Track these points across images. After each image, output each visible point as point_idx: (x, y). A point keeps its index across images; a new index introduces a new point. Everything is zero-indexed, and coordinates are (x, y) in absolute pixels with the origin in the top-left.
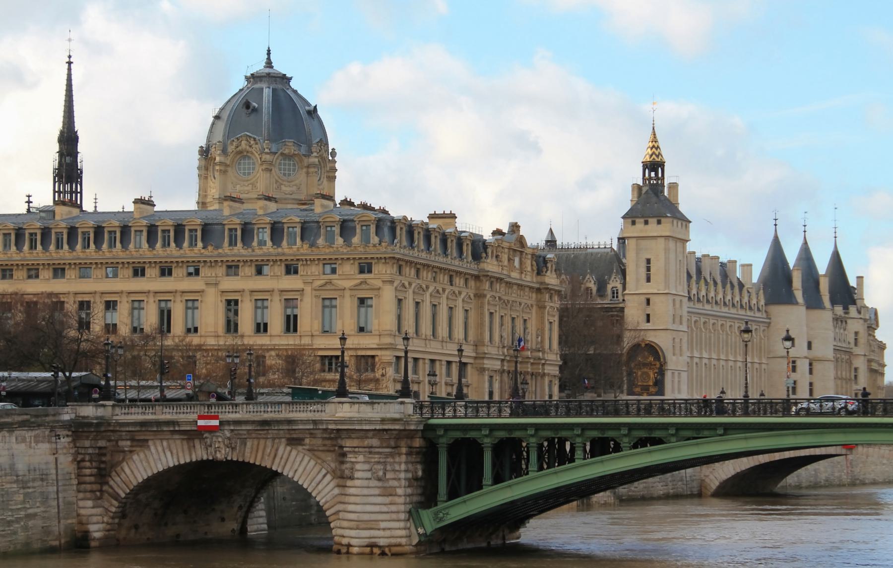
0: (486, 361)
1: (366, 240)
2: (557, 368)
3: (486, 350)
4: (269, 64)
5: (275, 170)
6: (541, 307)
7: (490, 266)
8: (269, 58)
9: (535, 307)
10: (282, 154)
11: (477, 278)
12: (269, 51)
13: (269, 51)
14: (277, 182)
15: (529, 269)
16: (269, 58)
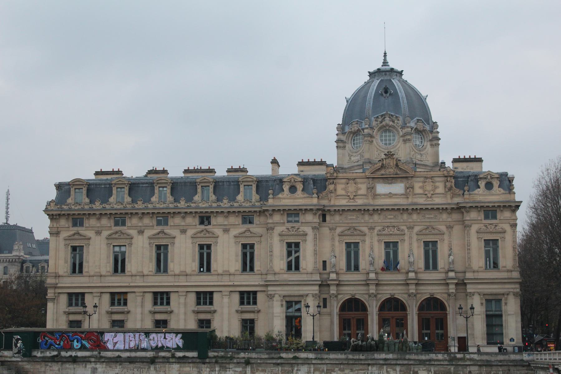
0: (270, 288)
1: (162, 200)
2: (518, 286)
3: (270, 277)
4: (385, 63)
5: (349, 146)
6: (466, 227)
7: (339, 196)
8: (385, 60)
9: (457, 229)
10: (351, 132)
11: (262, 213)
12: (385, 53)
13: (385, 53)
14: (349, 155)
15: (441, 189)
16: (385, 60)
